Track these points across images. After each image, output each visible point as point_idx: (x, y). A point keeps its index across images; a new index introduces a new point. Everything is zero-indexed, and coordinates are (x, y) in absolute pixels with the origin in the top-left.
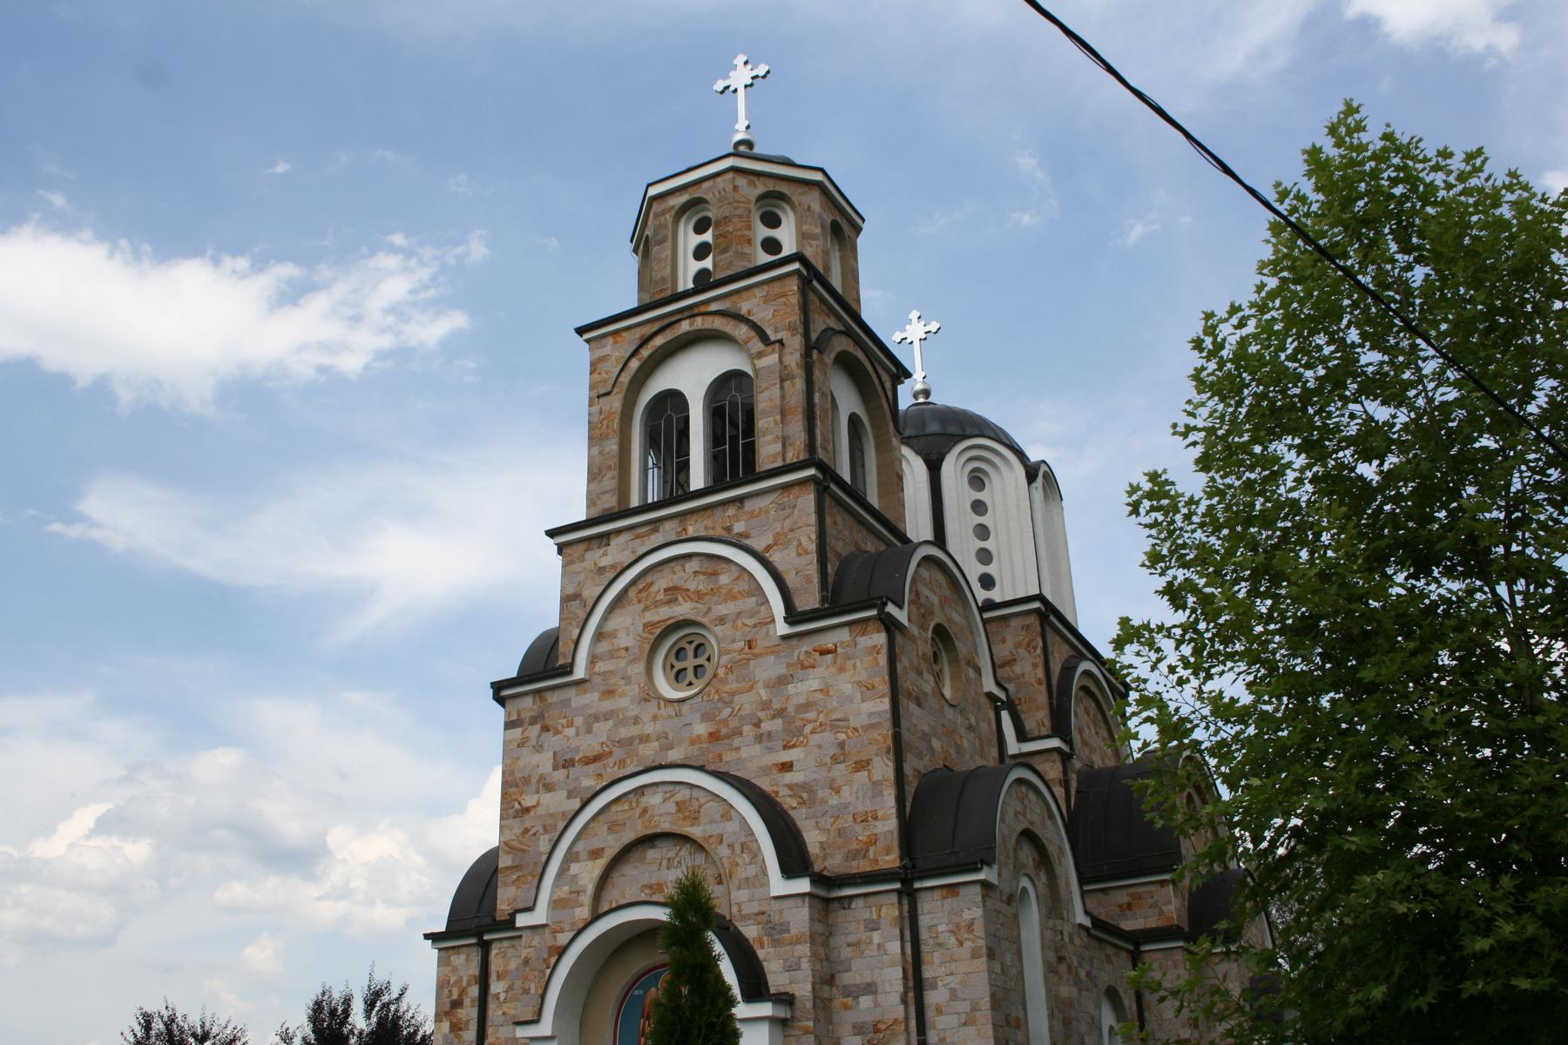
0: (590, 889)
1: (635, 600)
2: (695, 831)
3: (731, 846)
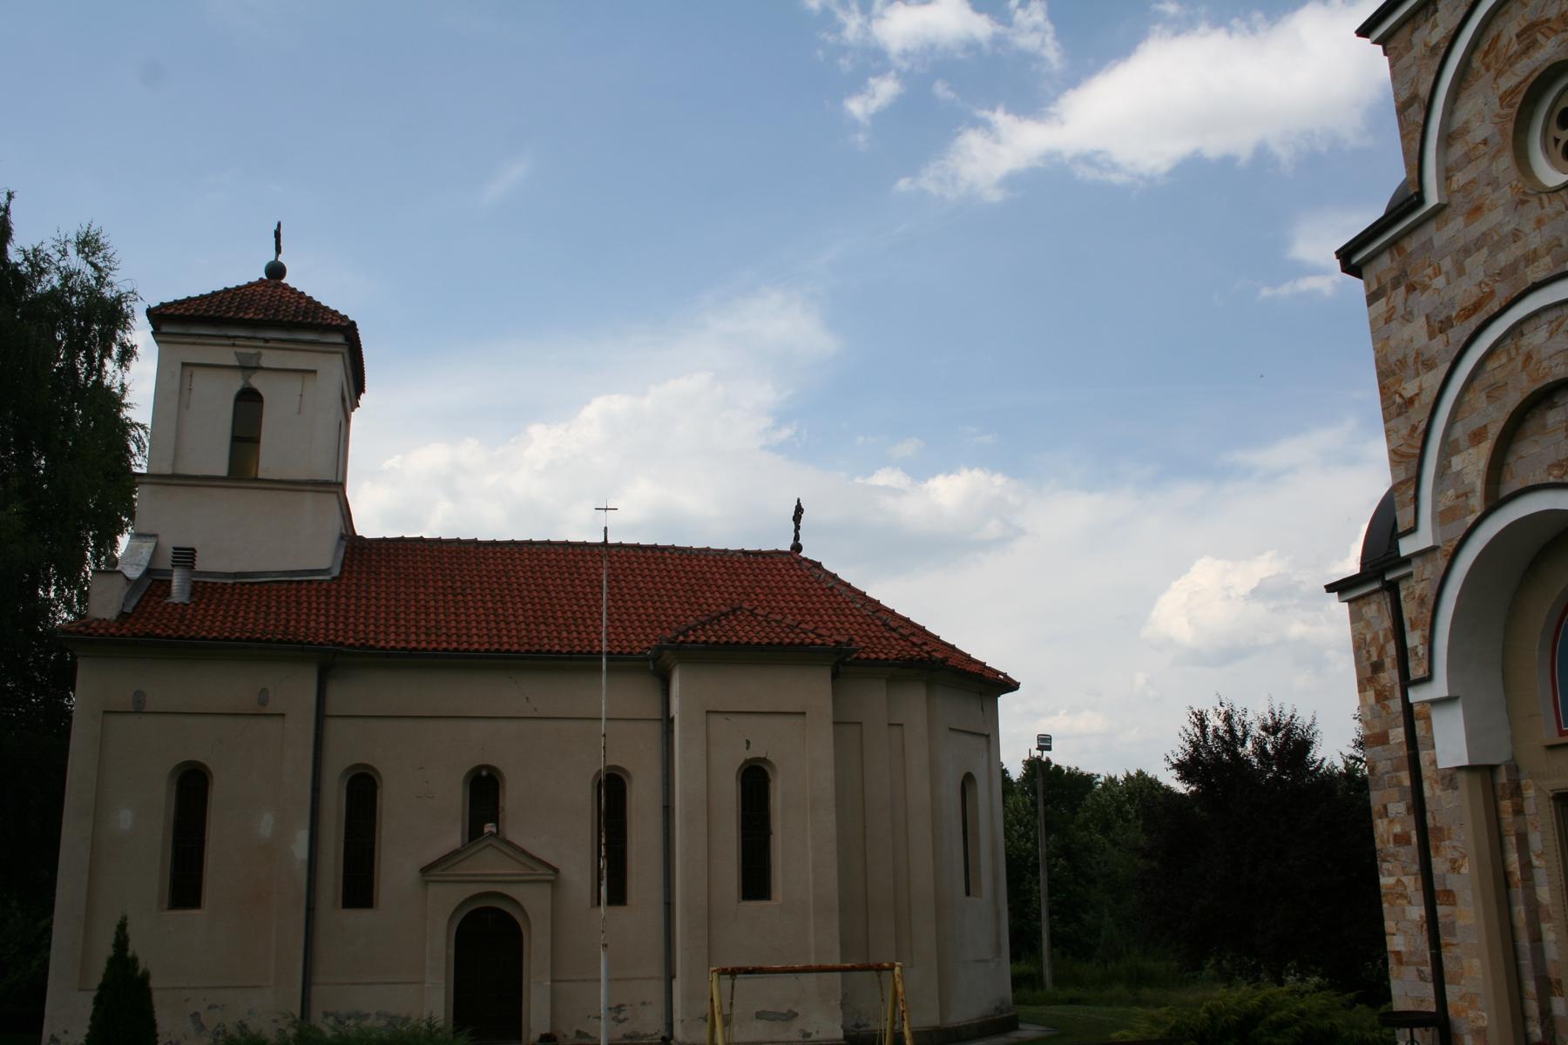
1: (1483, 70)
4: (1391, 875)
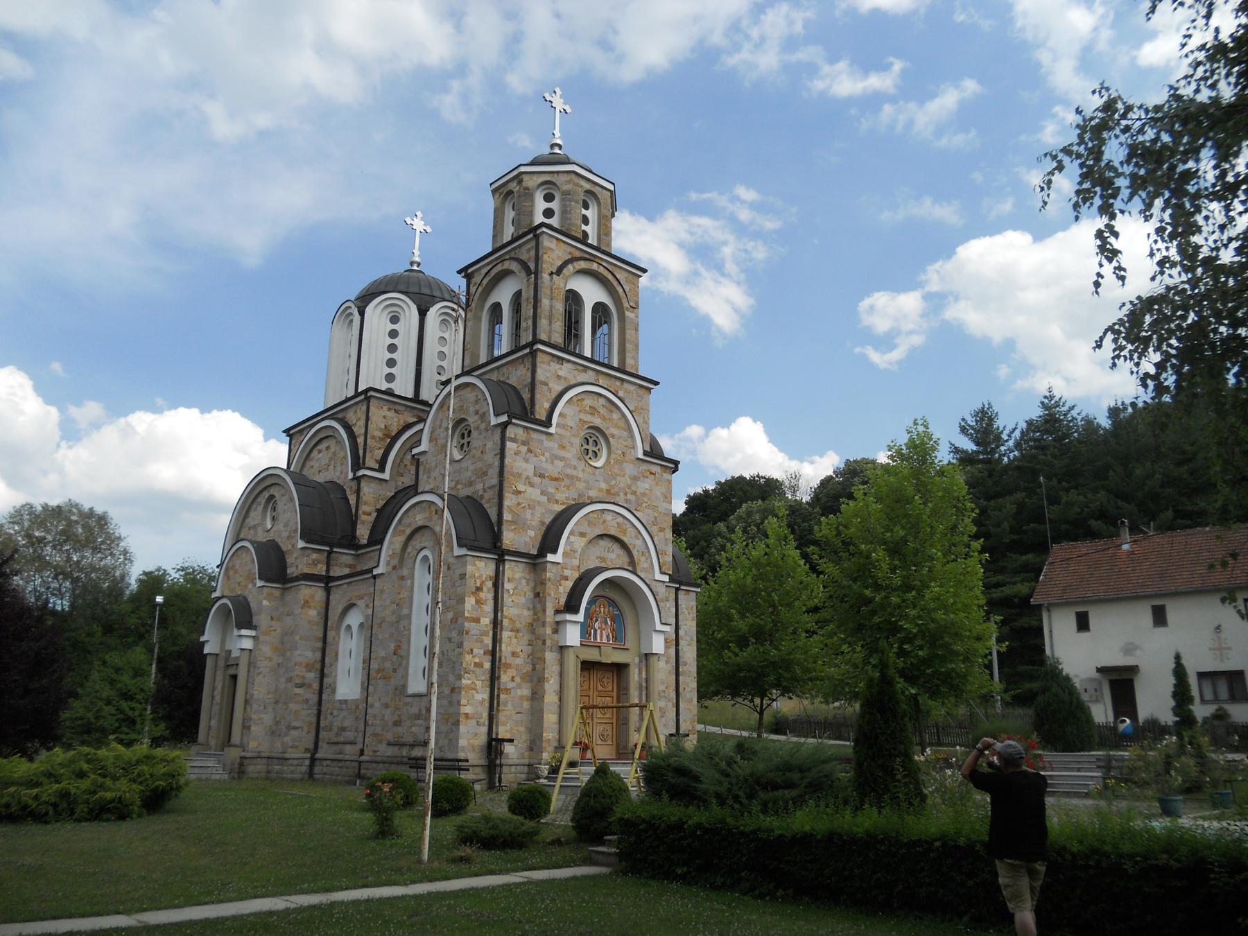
0: (579, 551)
2: (625, 539)
4: (469, 679)
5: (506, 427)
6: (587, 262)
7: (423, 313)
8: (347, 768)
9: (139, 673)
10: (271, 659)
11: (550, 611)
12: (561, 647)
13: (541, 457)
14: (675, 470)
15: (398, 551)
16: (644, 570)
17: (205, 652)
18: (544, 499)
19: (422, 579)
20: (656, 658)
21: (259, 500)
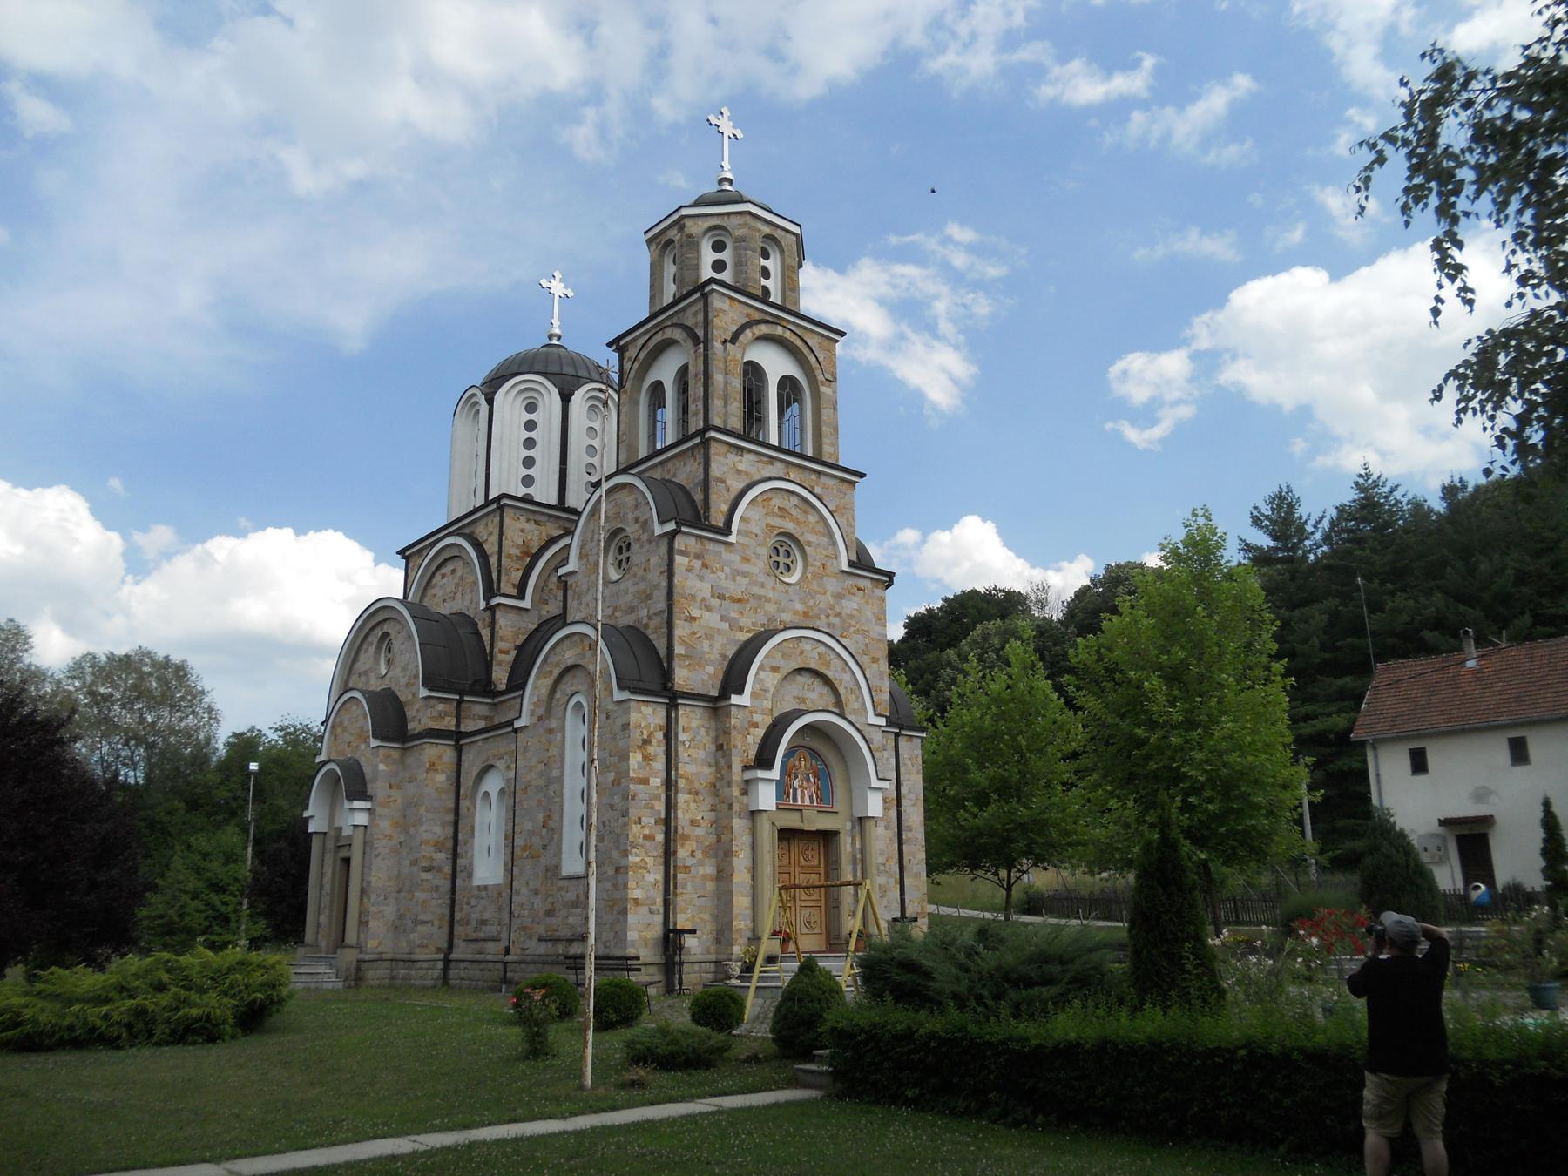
0: (772, 690)
2: (829, 674)
3: (846, 688)
4: (637, 855)
5: (674, 537)
6: (770, 325)
7: (566, 398)
8: (490, 970)
9: (231, 858)
10: (391, 838)
11: (737, 767)
12: (752, 812)
13: (720, 574)
14: (890, 584)
15: (545, 697)
16: (855, 712)
17: (310, 831)
18: (725, 626)
19: (575, 730)
20: (873, 822)
21: (370, 639)
